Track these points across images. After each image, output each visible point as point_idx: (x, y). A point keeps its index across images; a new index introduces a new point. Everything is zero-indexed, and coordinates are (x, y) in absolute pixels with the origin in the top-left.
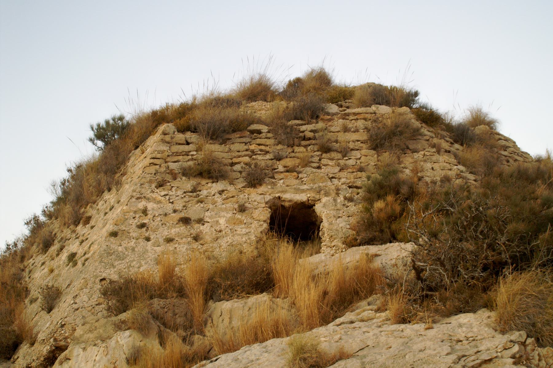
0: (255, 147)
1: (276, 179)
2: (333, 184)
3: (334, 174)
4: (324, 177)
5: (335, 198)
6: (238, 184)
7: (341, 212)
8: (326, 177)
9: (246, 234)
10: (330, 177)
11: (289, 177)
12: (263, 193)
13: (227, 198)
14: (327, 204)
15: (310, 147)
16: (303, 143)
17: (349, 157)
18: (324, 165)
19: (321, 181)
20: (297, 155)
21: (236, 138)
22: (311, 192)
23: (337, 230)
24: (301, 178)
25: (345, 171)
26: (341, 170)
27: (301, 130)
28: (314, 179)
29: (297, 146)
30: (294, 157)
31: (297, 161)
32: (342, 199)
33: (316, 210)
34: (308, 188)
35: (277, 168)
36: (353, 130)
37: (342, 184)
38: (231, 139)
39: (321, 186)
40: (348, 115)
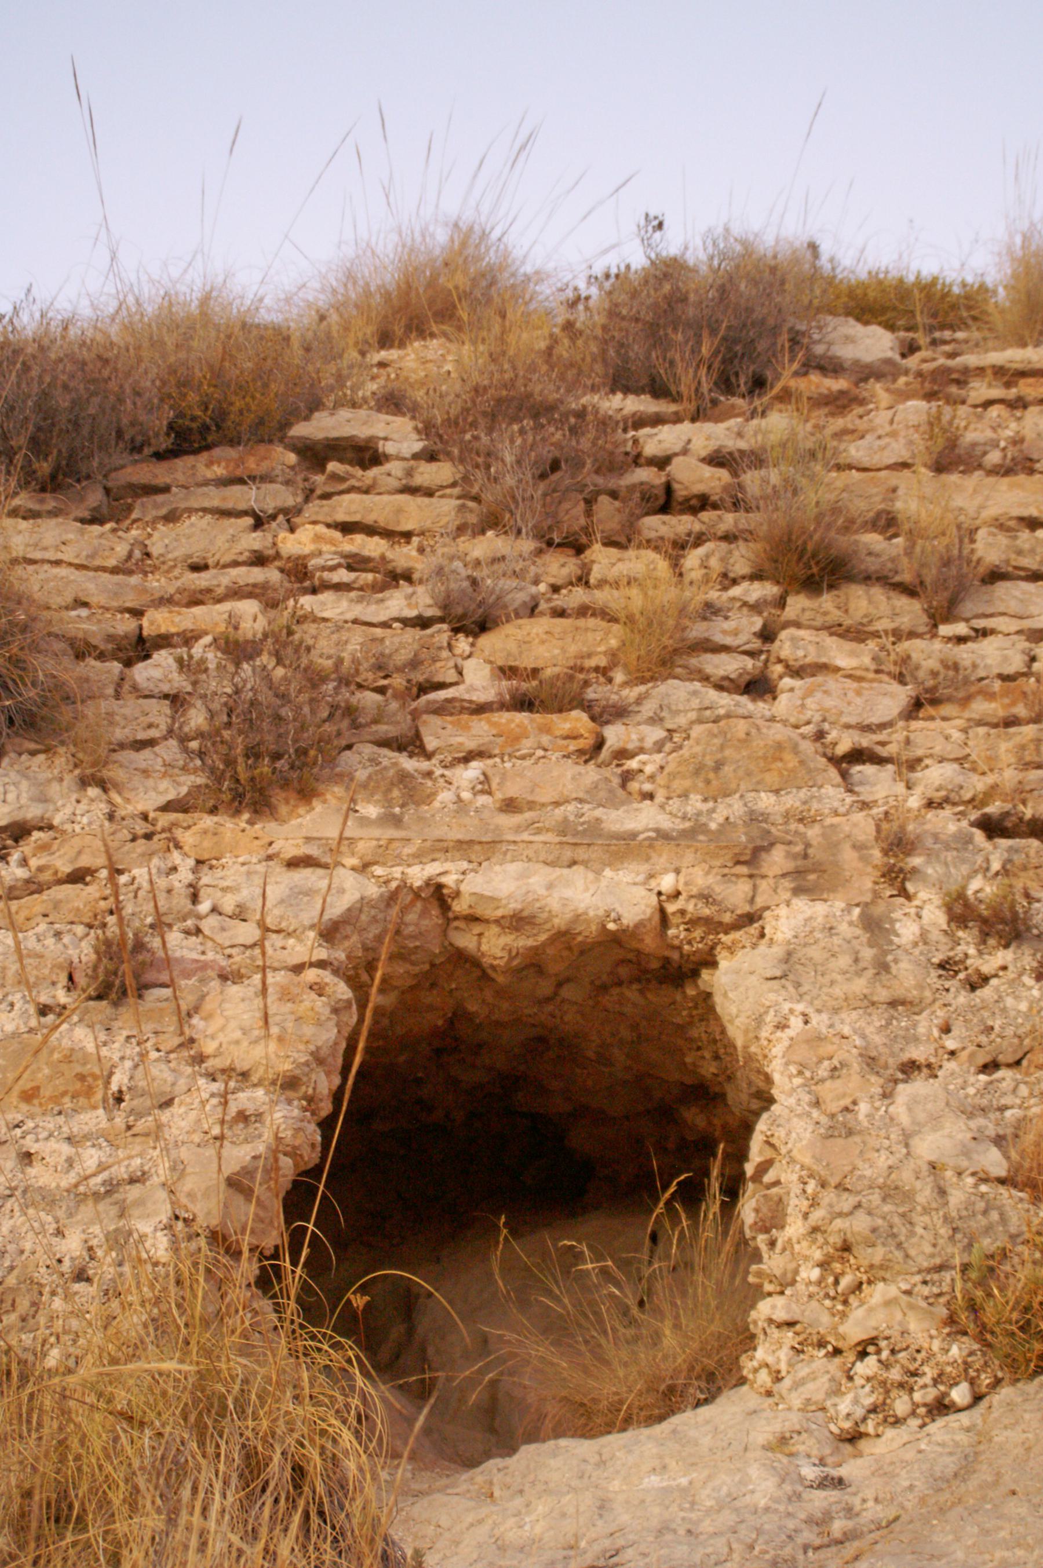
0: (318, 538)
1: (429, 756)
2: (865, 805)
3: (867, 728)
4: (795, 749)
5: (879, 909)
6: (137, 780)
7: (926, 1024)
8: (808, 747)
9: (97, 1196)
10: (842, 749)
11: (526, 746)
12: (313, 850)
13: (34, 886)
14: (815, 953)
15: (701, 551)
16: (655, 525)
17: (980, 623)
18: (797, 672)
19: (772, 779)
20: (601, 597)
21: (206, 483)
22: (689, 857)
23: (891, 1192)
24: (622, 754)
25: (947, 710)
26: (917, 704)
27: (650, 449)
28: (718, 766)
29: (610, 543)
30: (583, 611)
31: (613, 637)
32: (935, 916)
33: (718, 999)
34: (665, 822)
35: (451, 676)
36: (994, 457)
37: (930, 804)
38: (166, 489)
39: (765, 817)
40: (963, 378)
